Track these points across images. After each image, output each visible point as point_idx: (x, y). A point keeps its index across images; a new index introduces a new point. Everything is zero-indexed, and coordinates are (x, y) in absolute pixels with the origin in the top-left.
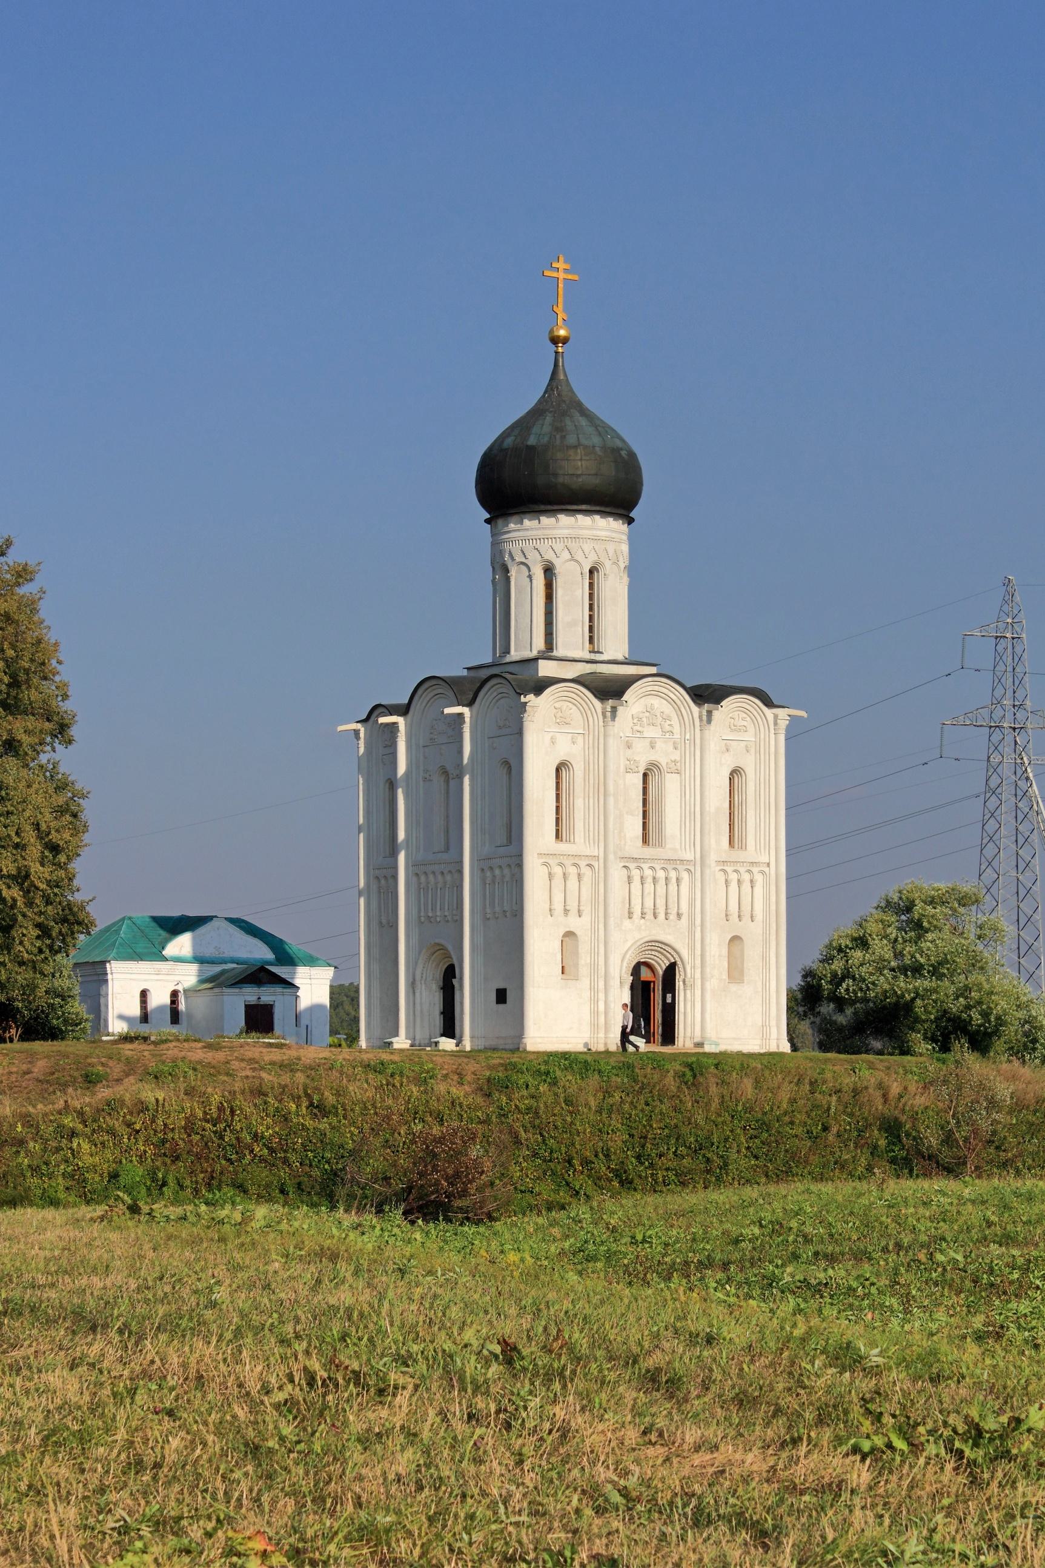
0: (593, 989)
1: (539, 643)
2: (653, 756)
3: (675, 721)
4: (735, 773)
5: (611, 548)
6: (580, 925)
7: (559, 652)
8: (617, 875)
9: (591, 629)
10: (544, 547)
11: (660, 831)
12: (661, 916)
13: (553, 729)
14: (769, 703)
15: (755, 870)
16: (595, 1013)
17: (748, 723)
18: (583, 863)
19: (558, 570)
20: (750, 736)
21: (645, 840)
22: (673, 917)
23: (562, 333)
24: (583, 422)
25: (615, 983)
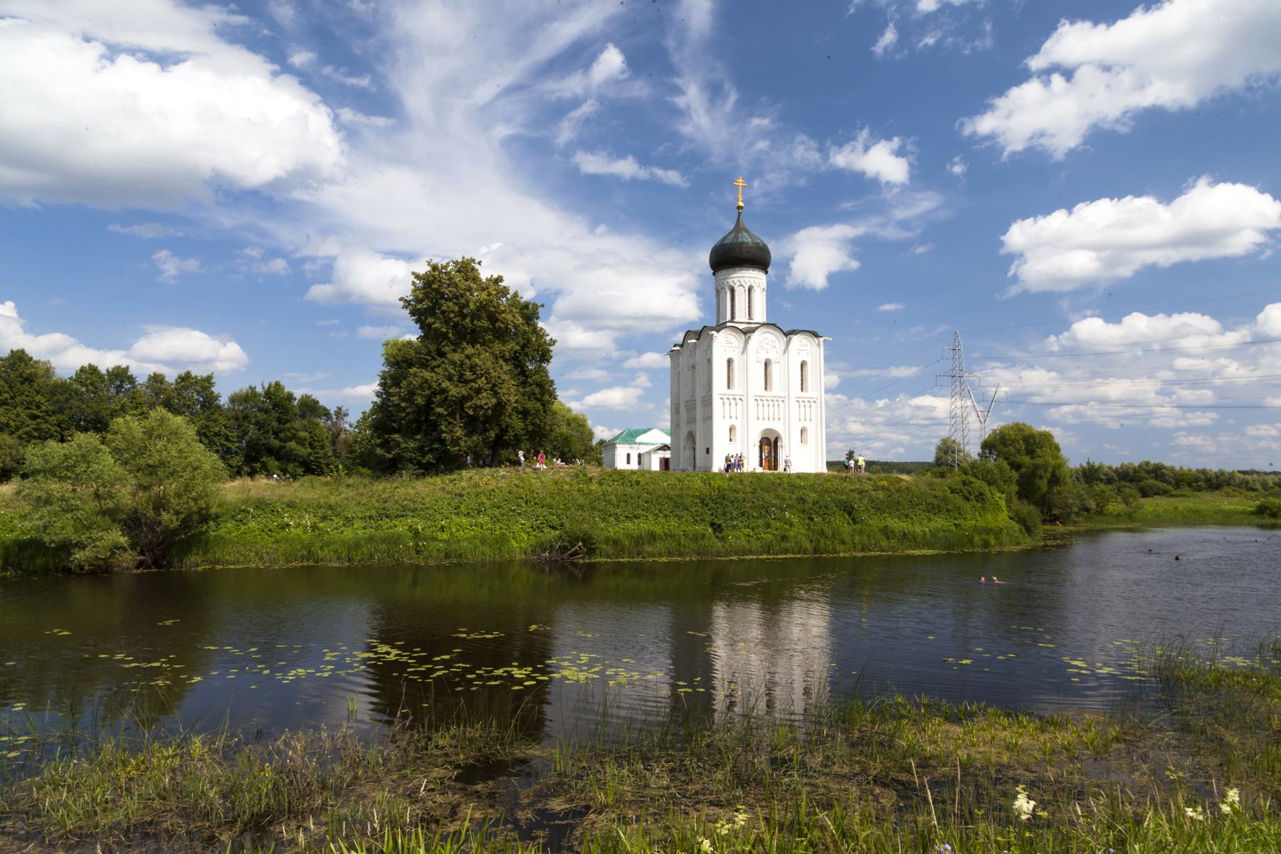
1: (729, 317)
4: (803, 365)
6: (738, 424)
13: (723, 345)
14: (816, 335)
19: (736, 288)
23: (741, 204)
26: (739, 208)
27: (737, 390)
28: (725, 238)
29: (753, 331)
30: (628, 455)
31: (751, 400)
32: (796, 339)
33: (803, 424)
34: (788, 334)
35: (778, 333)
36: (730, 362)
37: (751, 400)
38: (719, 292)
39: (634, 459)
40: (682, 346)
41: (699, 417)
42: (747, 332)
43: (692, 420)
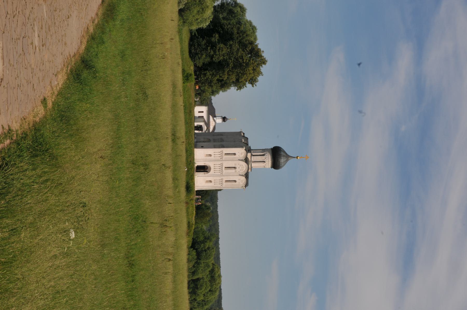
2: (237, 168)
4: (235, 181)
7: (252, 157)
8: (220, 163)
13: (240, 152)
14: (246, 186)
24: (285, 160)
26: (297, 157)
27: (225, 157)
28: (284, 152)
30: (203, 112)
32: (244, 179)
33: (213, 181)
34: (247, 176)
36: (235, 154)
38: (264, 150)
39: (201, 115)
40: (244, 136)
41: (215, 143)
43: (215, 141)
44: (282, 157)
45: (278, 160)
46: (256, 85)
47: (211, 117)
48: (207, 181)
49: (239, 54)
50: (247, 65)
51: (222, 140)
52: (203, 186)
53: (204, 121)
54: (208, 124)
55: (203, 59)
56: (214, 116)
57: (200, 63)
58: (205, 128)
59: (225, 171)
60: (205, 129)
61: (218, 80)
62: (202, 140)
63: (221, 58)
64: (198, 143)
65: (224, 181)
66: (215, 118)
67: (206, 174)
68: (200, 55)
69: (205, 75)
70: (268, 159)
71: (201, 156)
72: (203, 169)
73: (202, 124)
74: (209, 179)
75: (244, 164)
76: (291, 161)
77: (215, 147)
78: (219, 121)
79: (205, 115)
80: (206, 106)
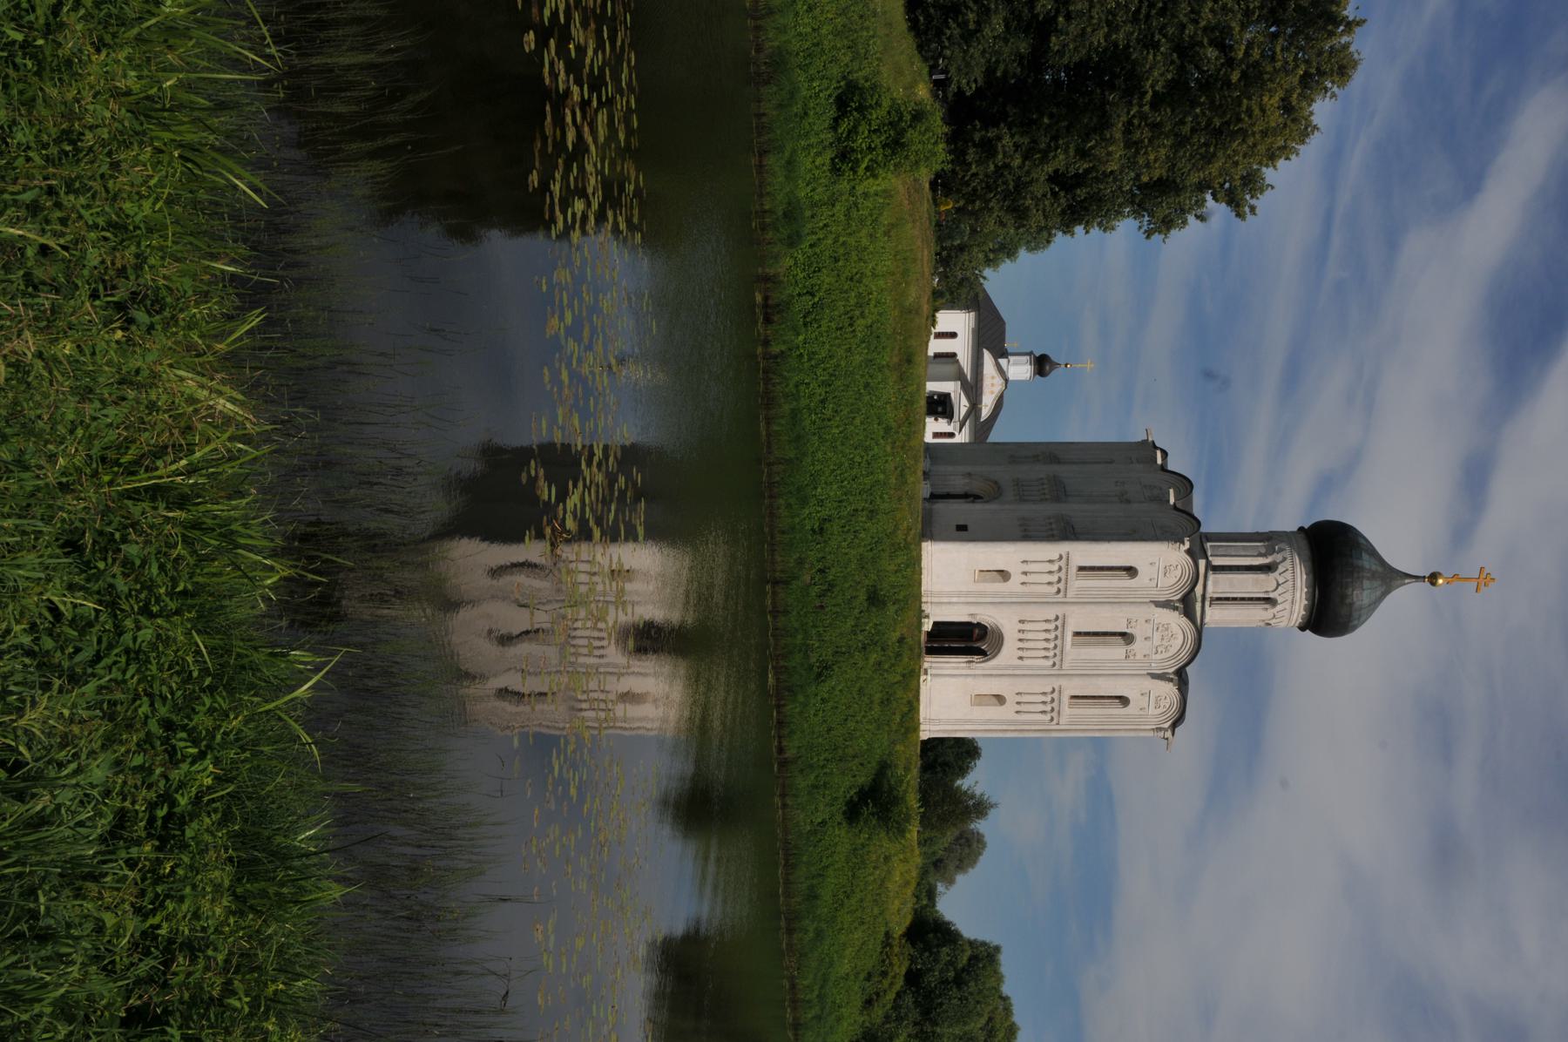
0: (968, 594)
1: (1217, 561)
3: (1165, 655)
4: (1124, 701)
5: (1286, 613)
6: (1014, 584)
7: (1211, 577)
9: (1227, 599)
10: (1287, 564)
11: (1084, 644)
12: (1021, 645)
13: (1161, 562)
14: (1174, 725)
15: (1055, 714)
16: (950, 595)
17: (1161, 710)
18: (1061, 585)
19: (1272, 576)
20: (1152, 711)
21: (1077, 634)
22: (1021, 653)
24: (1379, 593)
25: (973, 610)
26: (1433, 578)
27: (1078, 584)
28: (1373, 553)
29: (1188, 613)
30: (953, 335)
31: (1059, 610)
32: (1169, 690)
33: (1011, 698)
35: (1184, 656)
36: (1131, 571)
37: (1059, 610)
38: (1270, 540)
40: (1163, 468)
41: (1027, 509)
42: (1187, 605)
44: (1366, 584)
45: (1343, 597)
46: (1253, 209)
47: (988, 357)
48: (980, 700)
49: (1207, 16)
50: (1254, 78)
51: (1058, 491)
52: (958, 722)
53: (960, 376)
54: (973, 389)
55: (994, 44)
56: (1000, 353)
57: (968, 82)
58: (962, 405)
59: (1075, 654)
60: (964, 411)
61: (1055, 178)
62: (958, 484)
63: (1098, 38)
64: (940, 506)
65: (1065, 699)
66: (1003, 362)
67: (980, 666)
68: (971, 16)
69: (988, 148)
70: (1292, 588)
71: (951, 576)
72: (965, 640)
73: (949, 387)
74: (994, 686)
75: (1176, 622)
76: (1402, 596)
77: (1026, 533)
78: (1020, 370)
79: (961, 347)
80: (966, 307)
